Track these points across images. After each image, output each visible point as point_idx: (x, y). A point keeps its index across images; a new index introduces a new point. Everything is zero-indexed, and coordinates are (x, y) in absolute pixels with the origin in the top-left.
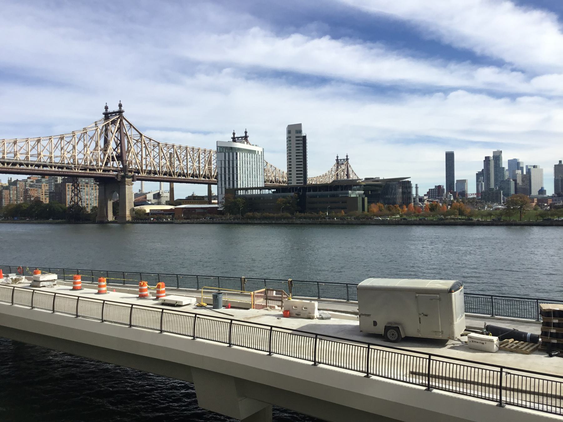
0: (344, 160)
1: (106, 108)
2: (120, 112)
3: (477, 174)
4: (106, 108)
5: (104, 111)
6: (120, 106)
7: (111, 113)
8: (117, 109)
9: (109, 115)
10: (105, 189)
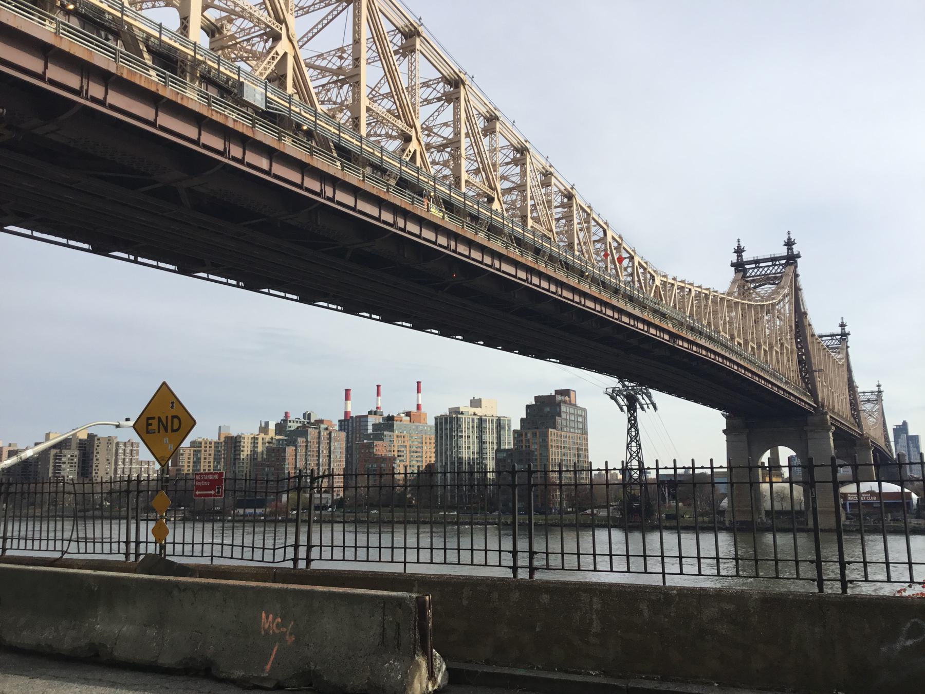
0: (872, 392)
1: (739, 251)
2: (791, 259)
3: (894, 429)
4: (739, 251)
5: (734, 257)
6: (789, 244)
7: (756, 262)
8: (783, 251)
9: (753, 266)
10: (749, 444)
